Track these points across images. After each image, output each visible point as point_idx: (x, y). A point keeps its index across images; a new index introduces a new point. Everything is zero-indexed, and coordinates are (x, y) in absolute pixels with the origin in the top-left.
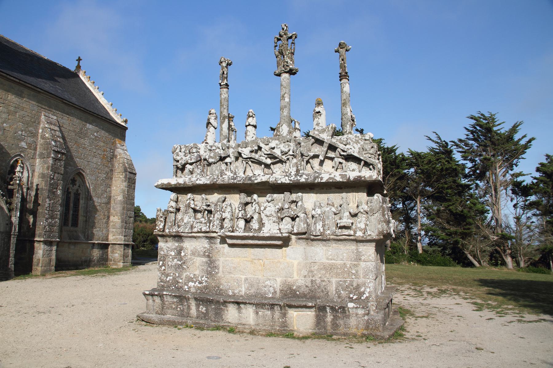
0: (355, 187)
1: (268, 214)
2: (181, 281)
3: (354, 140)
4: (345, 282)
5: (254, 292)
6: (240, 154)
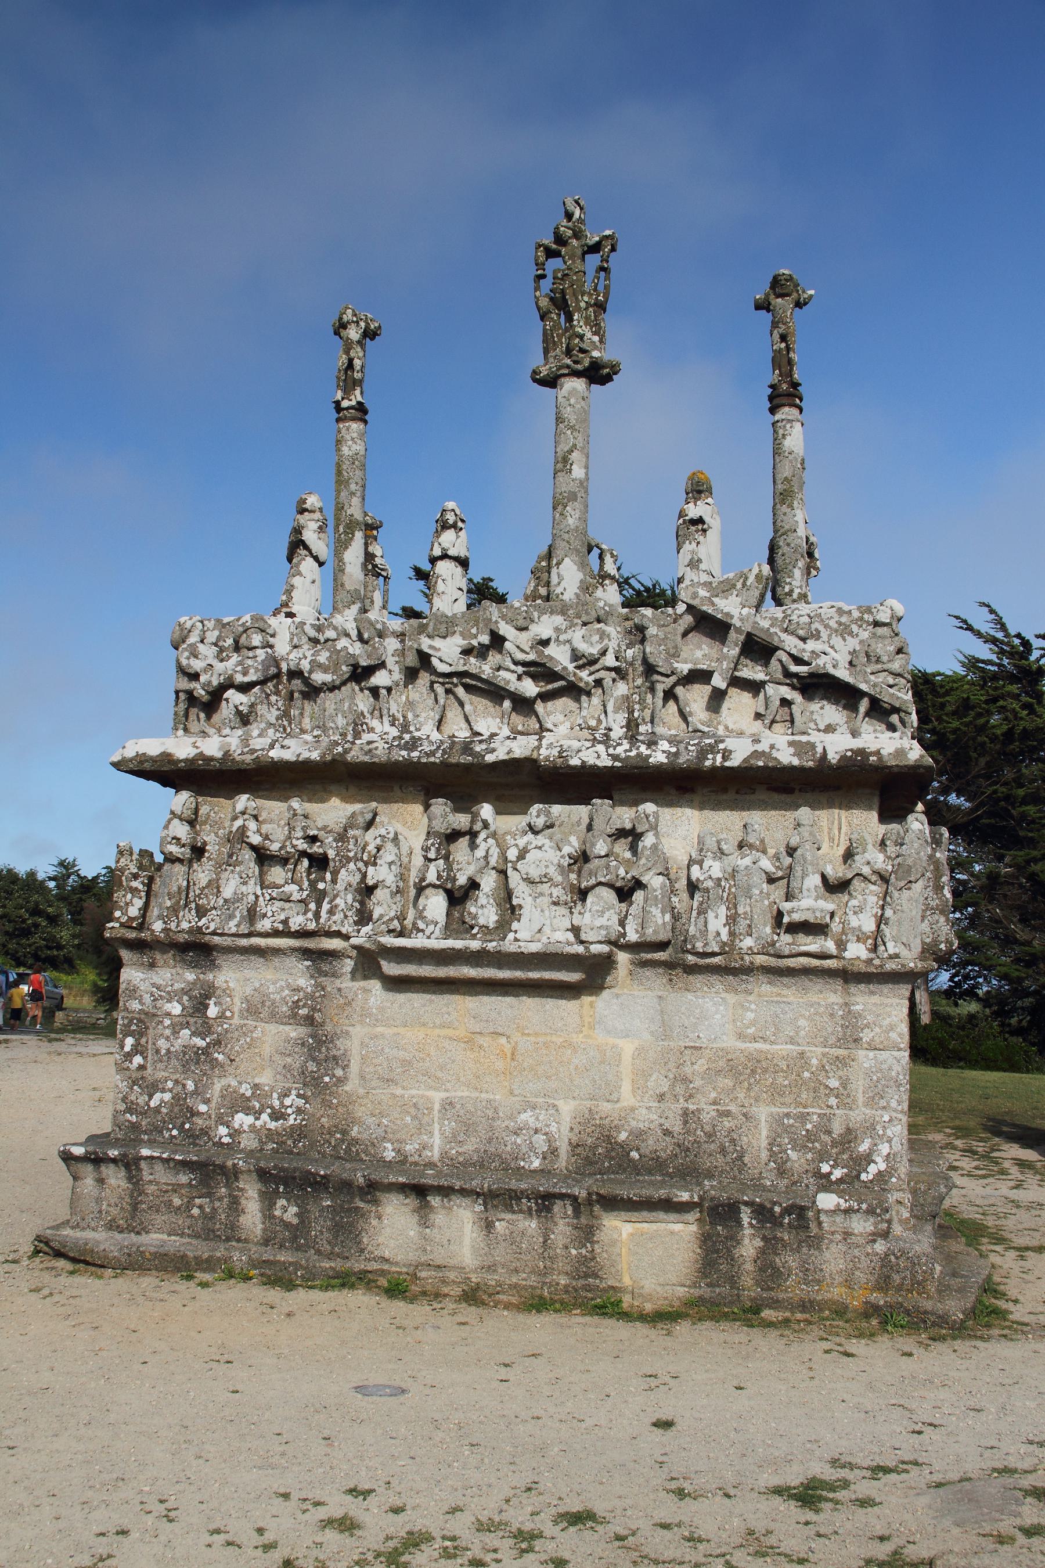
0: (837, 788)
1: (535, 874)
2: (203, 1108)
3: (833, 624)
4: (803, 1118)
5: (477, 1150)
6: (424, 658)
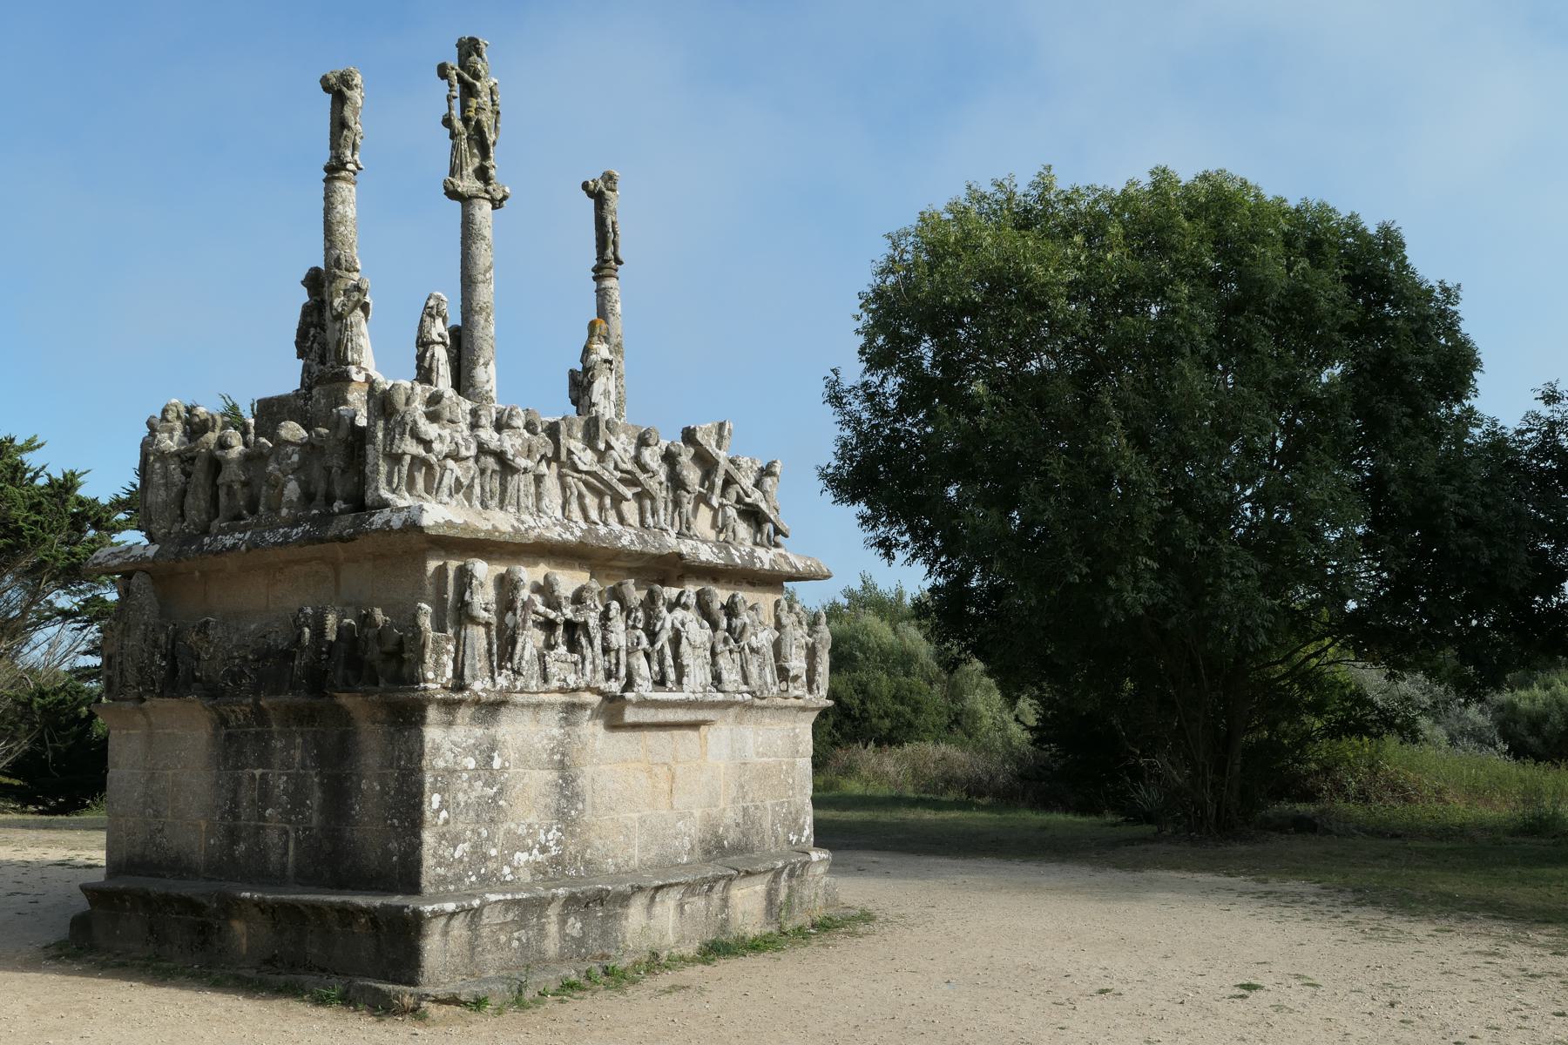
2: (493, 852)
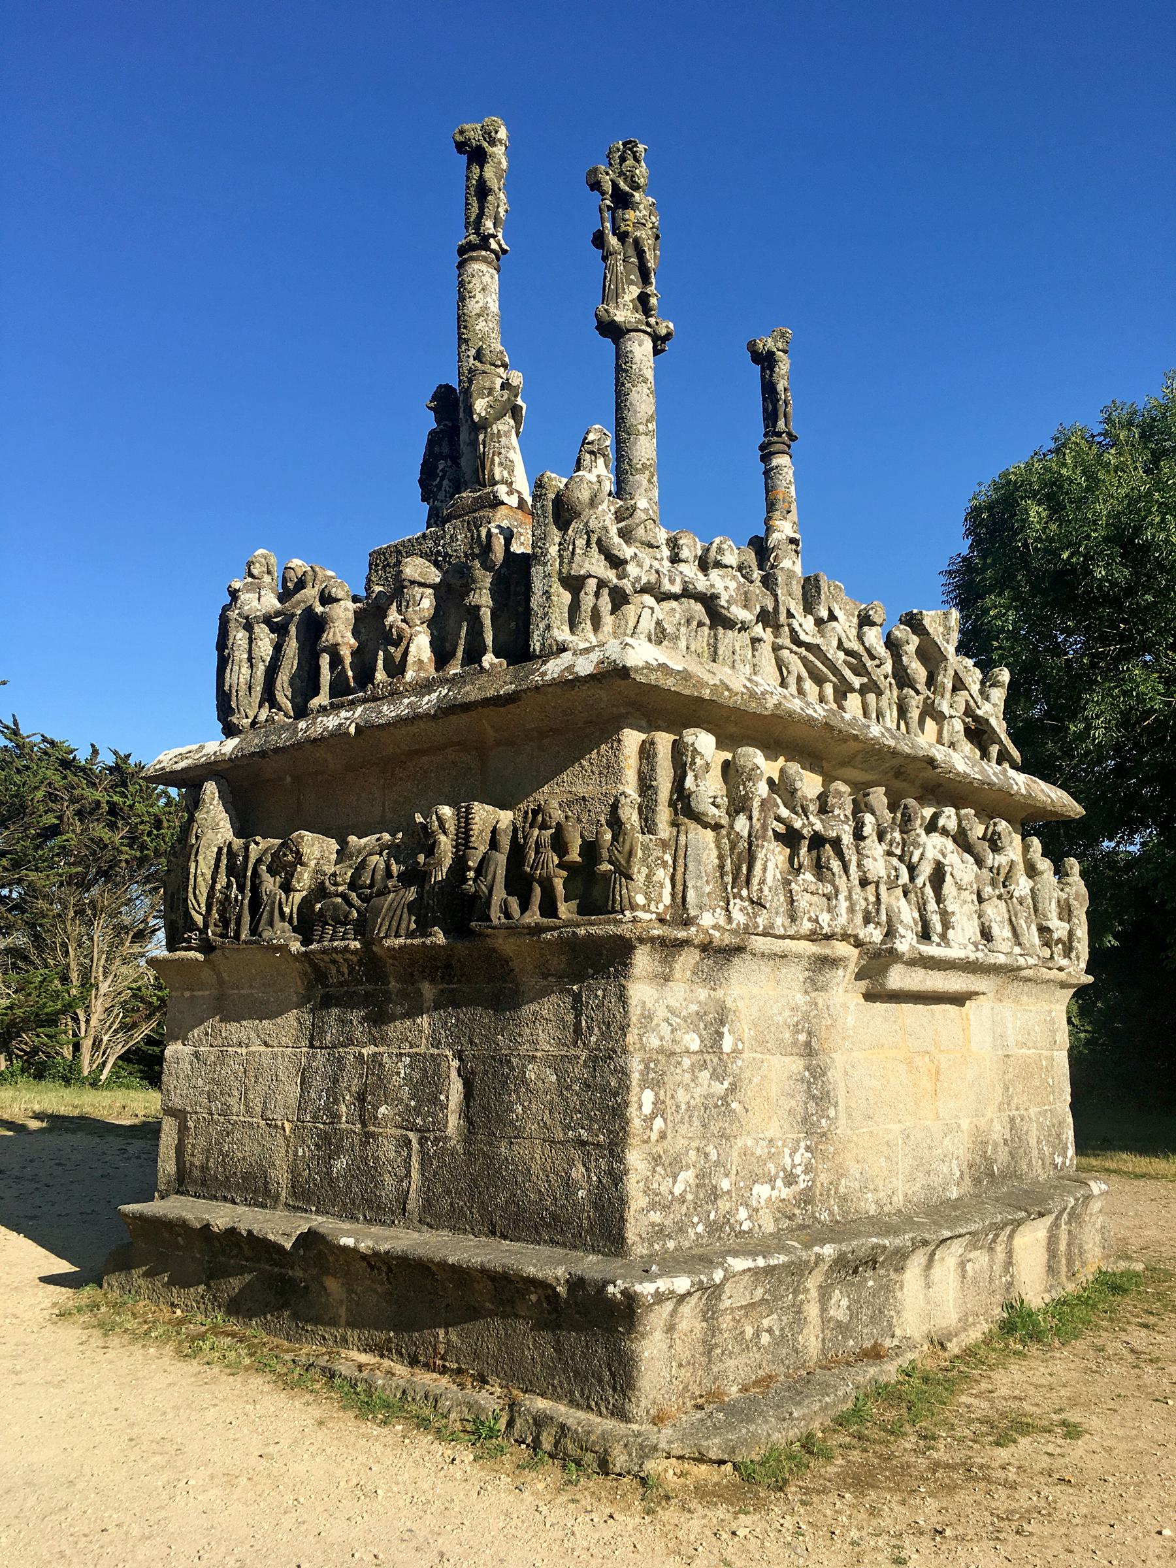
2: (725, 1184)
